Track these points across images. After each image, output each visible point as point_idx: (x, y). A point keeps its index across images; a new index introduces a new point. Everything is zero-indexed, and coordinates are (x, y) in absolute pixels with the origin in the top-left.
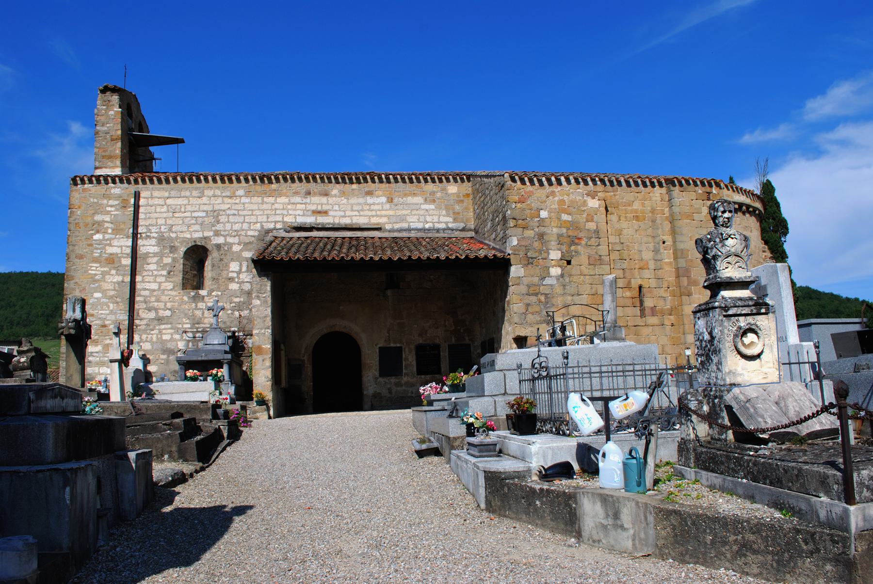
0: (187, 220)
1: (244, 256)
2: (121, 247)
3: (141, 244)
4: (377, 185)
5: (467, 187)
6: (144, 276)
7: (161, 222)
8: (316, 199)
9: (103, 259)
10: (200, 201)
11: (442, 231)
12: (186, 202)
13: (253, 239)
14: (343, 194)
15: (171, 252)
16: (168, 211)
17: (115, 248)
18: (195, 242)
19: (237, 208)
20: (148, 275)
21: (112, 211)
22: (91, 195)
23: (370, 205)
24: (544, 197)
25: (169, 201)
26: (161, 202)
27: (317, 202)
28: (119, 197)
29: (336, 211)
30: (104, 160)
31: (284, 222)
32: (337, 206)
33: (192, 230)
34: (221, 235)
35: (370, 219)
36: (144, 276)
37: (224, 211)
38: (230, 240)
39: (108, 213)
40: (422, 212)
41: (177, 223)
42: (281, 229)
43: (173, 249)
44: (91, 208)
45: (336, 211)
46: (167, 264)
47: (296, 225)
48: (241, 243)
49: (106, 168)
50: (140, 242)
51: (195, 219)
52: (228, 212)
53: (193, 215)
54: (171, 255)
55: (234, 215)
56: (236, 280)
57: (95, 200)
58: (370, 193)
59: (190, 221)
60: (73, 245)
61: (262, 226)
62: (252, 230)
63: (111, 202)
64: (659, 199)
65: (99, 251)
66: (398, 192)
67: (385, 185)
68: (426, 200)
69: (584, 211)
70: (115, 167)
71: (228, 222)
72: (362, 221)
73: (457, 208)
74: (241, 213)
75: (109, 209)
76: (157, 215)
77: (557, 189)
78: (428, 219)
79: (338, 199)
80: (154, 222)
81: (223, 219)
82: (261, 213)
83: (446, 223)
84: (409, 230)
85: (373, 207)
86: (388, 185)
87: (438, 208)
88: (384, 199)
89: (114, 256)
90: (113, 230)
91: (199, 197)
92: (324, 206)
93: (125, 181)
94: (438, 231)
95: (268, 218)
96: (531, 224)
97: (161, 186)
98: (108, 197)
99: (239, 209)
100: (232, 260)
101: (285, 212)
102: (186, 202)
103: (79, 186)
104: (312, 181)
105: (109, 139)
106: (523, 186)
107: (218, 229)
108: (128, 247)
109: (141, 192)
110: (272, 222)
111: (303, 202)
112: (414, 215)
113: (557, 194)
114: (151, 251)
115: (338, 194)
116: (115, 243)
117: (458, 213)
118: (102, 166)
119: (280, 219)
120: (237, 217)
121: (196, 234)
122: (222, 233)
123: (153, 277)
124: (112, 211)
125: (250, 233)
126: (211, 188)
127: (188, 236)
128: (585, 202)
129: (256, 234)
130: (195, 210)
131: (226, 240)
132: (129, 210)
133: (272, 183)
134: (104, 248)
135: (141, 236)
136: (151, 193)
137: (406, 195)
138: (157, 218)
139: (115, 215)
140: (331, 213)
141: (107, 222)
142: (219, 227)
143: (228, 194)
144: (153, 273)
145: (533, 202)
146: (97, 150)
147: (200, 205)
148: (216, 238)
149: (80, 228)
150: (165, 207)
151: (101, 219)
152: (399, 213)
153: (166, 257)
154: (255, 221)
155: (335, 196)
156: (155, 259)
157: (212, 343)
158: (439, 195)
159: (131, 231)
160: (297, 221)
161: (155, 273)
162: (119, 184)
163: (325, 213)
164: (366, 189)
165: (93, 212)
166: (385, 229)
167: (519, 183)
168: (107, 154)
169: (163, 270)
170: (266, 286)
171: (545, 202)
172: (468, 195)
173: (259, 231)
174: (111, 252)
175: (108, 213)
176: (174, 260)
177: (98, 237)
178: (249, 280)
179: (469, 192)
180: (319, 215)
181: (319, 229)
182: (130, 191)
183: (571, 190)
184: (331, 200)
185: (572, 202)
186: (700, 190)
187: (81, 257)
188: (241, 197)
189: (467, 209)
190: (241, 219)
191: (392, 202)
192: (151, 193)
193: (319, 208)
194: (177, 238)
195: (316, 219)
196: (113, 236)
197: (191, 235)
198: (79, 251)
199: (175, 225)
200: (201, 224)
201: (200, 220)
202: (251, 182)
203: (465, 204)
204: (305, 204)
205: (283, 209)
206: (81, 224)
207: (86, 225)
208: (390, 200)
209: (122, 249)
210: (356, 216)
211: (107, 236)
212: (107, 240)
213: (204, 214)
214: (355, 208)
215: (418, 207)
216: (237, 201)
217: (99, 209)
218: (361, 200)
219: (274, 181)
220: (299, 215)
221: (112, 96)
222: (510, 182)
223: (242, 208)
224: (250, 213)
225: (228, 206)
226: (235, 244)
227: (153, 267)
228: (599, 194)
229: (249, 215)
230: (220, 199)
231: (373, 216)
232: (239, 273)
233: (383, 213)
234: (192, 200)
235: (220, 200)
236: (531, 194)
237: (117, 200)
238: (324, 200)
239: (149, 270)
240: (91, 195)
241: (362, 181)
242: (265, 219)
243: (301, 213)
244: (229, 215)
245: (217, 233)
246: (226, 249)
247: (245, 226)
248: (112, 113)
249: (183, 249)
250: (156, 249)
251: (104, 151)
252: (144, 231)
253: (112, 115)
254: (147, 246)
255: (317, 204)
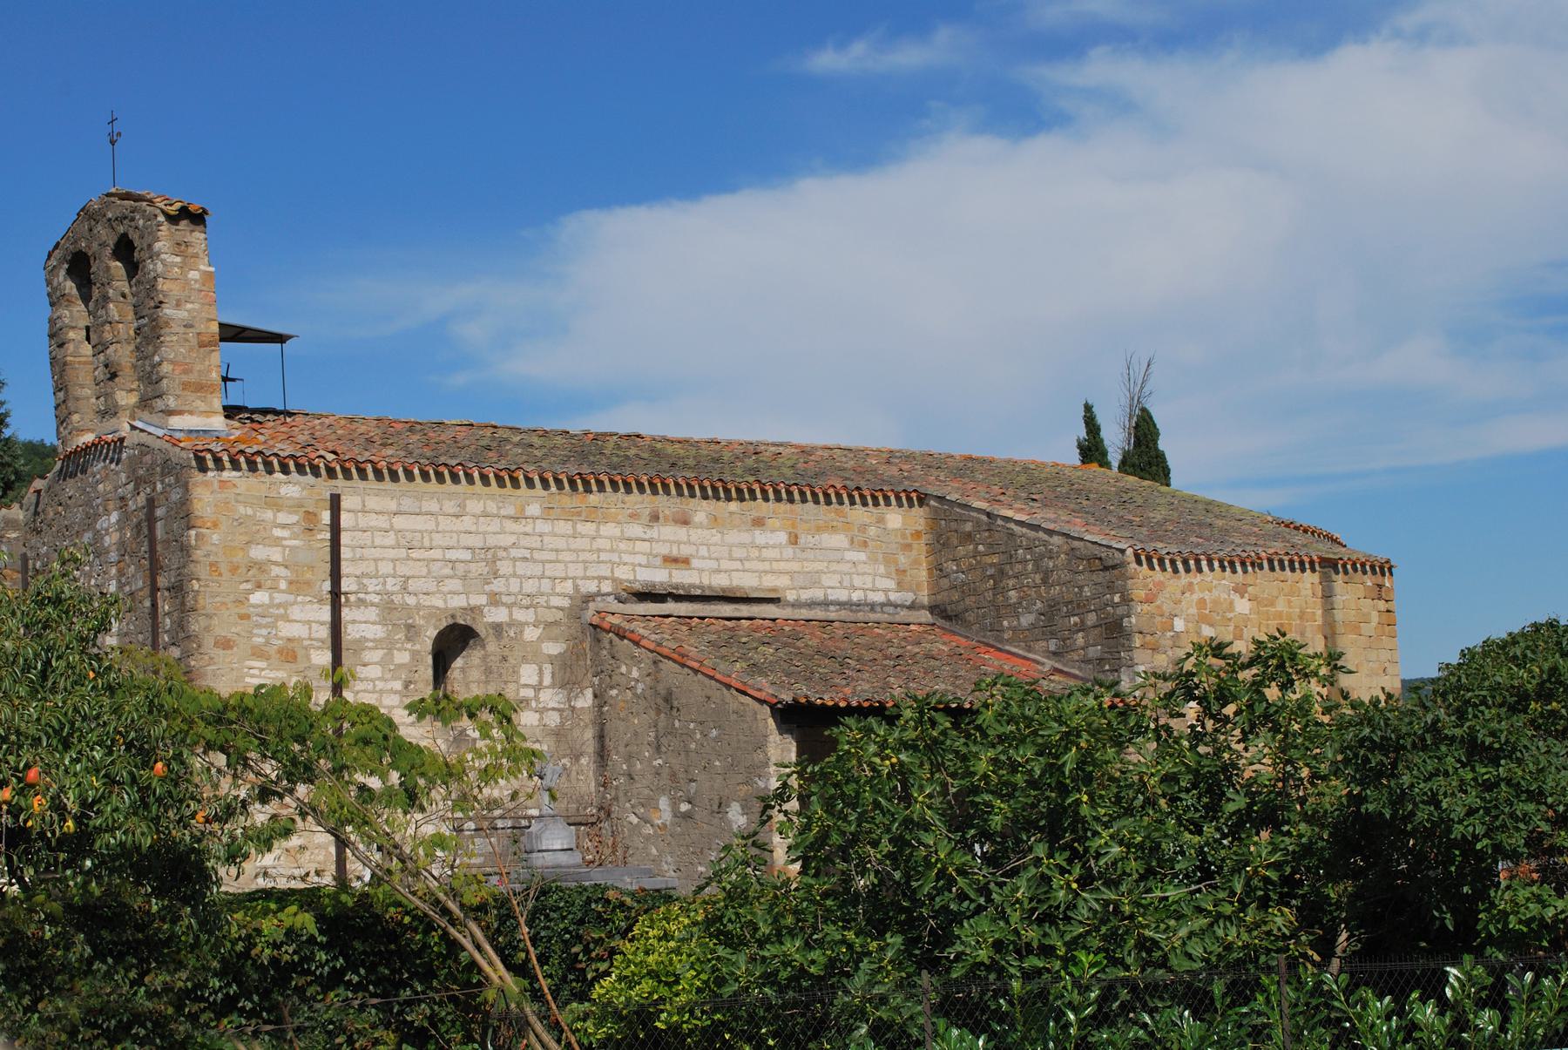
0: (435, 567)
1: (545, 651)
2: (309, 622)
3: (348, 618)
4: (772, 505)
5: (918, 517)
6: (358, 692)
7: (385, 568)
8: (669, 531)
9: (272, 651)
10: (459, 525)
11: (878, 609)
12: (431, 525)
13: (560, 615)
14: (714, 521)
15: (408, 639)
16: (398, 546)
17: (297, 625)
18: (453, 616)
19: (528, 545)
20: (365, 691)
21: (285, 539)
22: (240, 498)
23: (760, 548)
24: (1178, 592)
25: (399, 522)
26: (382, 522)
27: (670, 537)
28: (298, 505)
29: (704, 558)
30: (186, 393)
31: (614, 580)
32: (705, 548)
33: (445, 589)
34: (504, 604)
35: (760, 577)
36: (358, 692)
37: (505, 549)
38: (520, 615)
39: (277, 542)
40: (845, 567)
41: (417, 574)
42: (608, 594)
43: (412, 631)
44: (242, 529)
45: (704, 558)
46: (401, 666)
47: (637, 587)
48: (540, 623)
49: (191, 413)
50: (346, 614)
51: (450, 565)
52: (514, 553)
53: (447, 557)
54: (409, 646)
55: (525, 559)
56: (534, 704)
57: (250, 511)
58: (759, 523)
59: (441, 569)
60: (207, 615)
61: (576, 587)
62: (558, 595)
63: (283, 518)
64: (1310, 592)
65: (264, 632)
66: (806, 522)
67: (784, 507)
68: (852, 542)
69: (1230, 620)
70: (209, 413)
71: (514, 575)
72: (746, 582)
73: (903, 560)
74: (536, 555)
75: (278, 532)
76: (376, 553)
77: (1196, 578)
78: (857, 581)
79: (706, 532)
80: (371, 569)
81: (504, 567)
82: (573, 557)
83: (886, 591)
84: (826, 604)
85: (766, 553)
86: (789, 505)
87: (873, 560)
88: (782, 537)
89: (295, 644)
90: (291, 583)
91: (457, 516)
92: (682, 546)
93: (308, 470)
94: (872, 607)
95: (586, 569)
96: (1162, 642)
97: (380, 485)
98: (275, 504)
99: (534, 546)
100: (525, 660)
101: (615, 558)
102: (431, 525)
103: (210, 474)
104: (661, 492)
105: (194, 342)
106: (1151, 573)
107: (496, 589)
108: (322, 624)
109: (343, 497)
110: (594, 578)
111: (646, 537)
112: (834, 572)
113: (1196, 587)
114: (370, 636)
115: (705, 522)
116: (295, 613)
117: (904, 571)
118: (183, 408)
119: (608, 574)
120: (531, 565)
121: (453, 600)
122: (505, 599)
123: (376, 696)
124: (285, 539)
125: (556, 601)
126: (479, 496)
127: (440, 603)
128: (1232, 603)
129: (566, 603)
130: (451, 544)
131: (511, 614)
132: (319, 537)
133: (591, 492)
134: (274, 625)
135: (347, 600)
136: (363, 502)
137: (819, 529)
138: (375, 560)
139: (292, 548)
140: (695, 563)
141: (276, 563)
142: (497, 586)
143: (510, 511)
144: (374, 686)
145: (1164, 602)
146: (171, 367)
147: (459, 533)
148: (493, 609)
149: (220, 575)
150: (392, 533)
151: (264, 557)
152: (810, 566)
153: (398, 650)
154: (563, 575)
155: (701, 526)
156: (376, 655)
157: (551, 847)
158: (872, 531)
159: (327, 586)
160: (638, 578)
161: (380, 685)
162: (295, 475)
163: (684, 562)
164: (755, 514)
165: (246, 538)
166: (786, 601)
167: (1145, 566)
168: (193, 378)
169: (394, 678)
170: (790, 751)
171: (1180, 601)
172: (917, 534)
173: (571, 598)
174: (289, 635)
175: (277, 542)
176: (414, 654)
177: (259, 597)
178: (556, 706)
179: (920, 528)
180: (674, 566)
181: (678, 598)
182: (320, 494)
183: (1215, 582)
184: (696, 534)
185: (1216, 602)
186: (1369, 581)
187: (226, 644)
188: (534, 518)
189: (916, 562)
190: (537, 569)
191: (796, 543)
192: (363, 502)
193: (675, 553)
194: (418, 607)
195: (670, 576)
196: (291, 598)
197: (446, 602)
198: (221, 631)
199: (413, 577)
200: (464, 578)
201: (461, 568)
202: (554, 489)
203: (914, 552)
204: (650, 540)
205: (612, 551)
206: (223, 568)
207: (234, 569)
208: (793, 540)
209: (310, 628)
210: (737, 570)
211: (279, 598)
212: (279, 606)
213: (467, 555)
214: (738, 553)
215: (838, 555)
216: (529, 529)
217: (256, 534)
218: (745, 537)
219: (594, 488)
220: (640, 565)
221: (192, 231)
222: (1134, 565)
223: (538, 545)
224: (552, 556)
225: (513, 539)
226: (527, 624)
227: (374, 672)
228: (1250, 589)
229: (551, 562)
230: (497, 520)
231: (766, 572)
232: (538, 688)
233: (782, 566)
234: (445, 523)
235: (495, 525)
236: (1161, 586)
237: (296, 512)
238: (681, 532)
239: (366, 679)
240: (240, 498)
241: (747, 496)
242: (580, 573)
243: (642, 559)
244: (514, 560)
245: (494, 599)
246: (512, 634)
247: (546, 585)
248: (194, 275)
249: (432, 633)
250: (378, 631)
251: (186, 372)
252: (354, 588)
253: (196, 281)
254: (360, 624)
255: (672, 542)
